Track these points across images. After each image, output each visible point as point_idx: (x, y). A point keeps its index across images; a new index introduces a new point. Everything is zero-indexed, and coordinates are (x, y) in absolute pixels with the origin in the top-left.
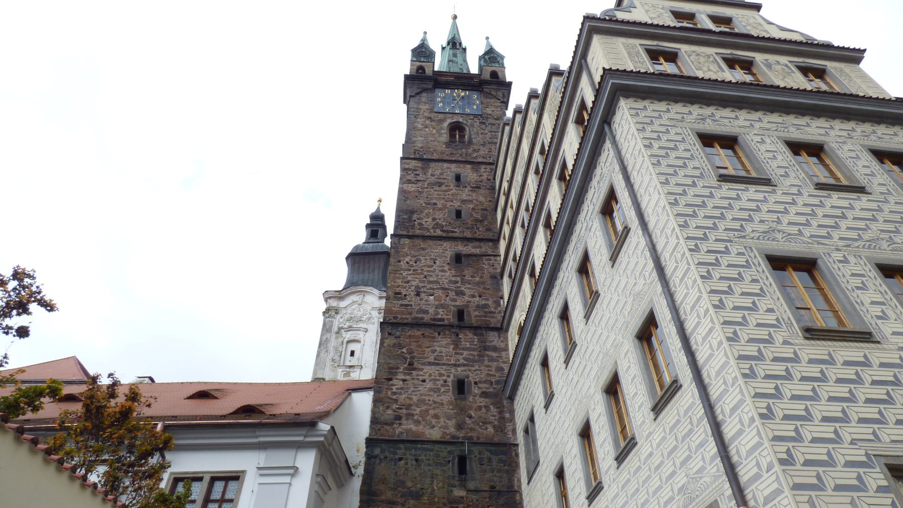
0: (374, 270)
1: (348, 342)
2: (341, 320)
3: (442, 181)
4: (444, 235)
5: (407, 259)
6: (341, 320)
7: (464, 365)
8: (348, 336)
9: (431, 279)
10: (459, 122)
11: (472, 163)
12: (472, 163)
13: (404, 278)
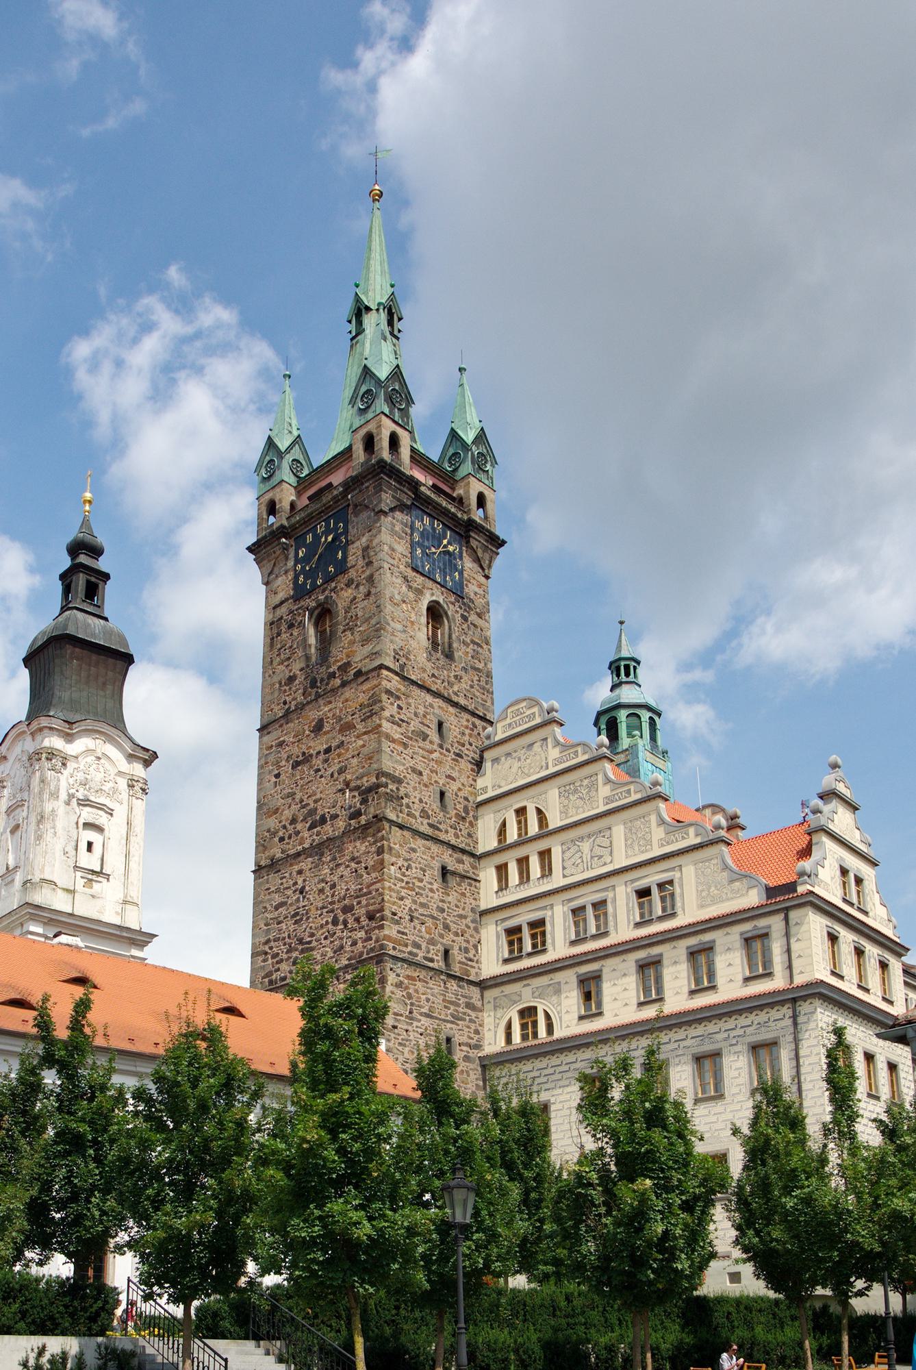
0: (104, 684)
1: (87, 825)
3: (425, 729)
4: (429, 831)
5: (400, 862)
6: (71, 781)
8: (87, 814)
10: (437, 602)
11: (456, 705)
12: (456, 705)
13: (398, 892)
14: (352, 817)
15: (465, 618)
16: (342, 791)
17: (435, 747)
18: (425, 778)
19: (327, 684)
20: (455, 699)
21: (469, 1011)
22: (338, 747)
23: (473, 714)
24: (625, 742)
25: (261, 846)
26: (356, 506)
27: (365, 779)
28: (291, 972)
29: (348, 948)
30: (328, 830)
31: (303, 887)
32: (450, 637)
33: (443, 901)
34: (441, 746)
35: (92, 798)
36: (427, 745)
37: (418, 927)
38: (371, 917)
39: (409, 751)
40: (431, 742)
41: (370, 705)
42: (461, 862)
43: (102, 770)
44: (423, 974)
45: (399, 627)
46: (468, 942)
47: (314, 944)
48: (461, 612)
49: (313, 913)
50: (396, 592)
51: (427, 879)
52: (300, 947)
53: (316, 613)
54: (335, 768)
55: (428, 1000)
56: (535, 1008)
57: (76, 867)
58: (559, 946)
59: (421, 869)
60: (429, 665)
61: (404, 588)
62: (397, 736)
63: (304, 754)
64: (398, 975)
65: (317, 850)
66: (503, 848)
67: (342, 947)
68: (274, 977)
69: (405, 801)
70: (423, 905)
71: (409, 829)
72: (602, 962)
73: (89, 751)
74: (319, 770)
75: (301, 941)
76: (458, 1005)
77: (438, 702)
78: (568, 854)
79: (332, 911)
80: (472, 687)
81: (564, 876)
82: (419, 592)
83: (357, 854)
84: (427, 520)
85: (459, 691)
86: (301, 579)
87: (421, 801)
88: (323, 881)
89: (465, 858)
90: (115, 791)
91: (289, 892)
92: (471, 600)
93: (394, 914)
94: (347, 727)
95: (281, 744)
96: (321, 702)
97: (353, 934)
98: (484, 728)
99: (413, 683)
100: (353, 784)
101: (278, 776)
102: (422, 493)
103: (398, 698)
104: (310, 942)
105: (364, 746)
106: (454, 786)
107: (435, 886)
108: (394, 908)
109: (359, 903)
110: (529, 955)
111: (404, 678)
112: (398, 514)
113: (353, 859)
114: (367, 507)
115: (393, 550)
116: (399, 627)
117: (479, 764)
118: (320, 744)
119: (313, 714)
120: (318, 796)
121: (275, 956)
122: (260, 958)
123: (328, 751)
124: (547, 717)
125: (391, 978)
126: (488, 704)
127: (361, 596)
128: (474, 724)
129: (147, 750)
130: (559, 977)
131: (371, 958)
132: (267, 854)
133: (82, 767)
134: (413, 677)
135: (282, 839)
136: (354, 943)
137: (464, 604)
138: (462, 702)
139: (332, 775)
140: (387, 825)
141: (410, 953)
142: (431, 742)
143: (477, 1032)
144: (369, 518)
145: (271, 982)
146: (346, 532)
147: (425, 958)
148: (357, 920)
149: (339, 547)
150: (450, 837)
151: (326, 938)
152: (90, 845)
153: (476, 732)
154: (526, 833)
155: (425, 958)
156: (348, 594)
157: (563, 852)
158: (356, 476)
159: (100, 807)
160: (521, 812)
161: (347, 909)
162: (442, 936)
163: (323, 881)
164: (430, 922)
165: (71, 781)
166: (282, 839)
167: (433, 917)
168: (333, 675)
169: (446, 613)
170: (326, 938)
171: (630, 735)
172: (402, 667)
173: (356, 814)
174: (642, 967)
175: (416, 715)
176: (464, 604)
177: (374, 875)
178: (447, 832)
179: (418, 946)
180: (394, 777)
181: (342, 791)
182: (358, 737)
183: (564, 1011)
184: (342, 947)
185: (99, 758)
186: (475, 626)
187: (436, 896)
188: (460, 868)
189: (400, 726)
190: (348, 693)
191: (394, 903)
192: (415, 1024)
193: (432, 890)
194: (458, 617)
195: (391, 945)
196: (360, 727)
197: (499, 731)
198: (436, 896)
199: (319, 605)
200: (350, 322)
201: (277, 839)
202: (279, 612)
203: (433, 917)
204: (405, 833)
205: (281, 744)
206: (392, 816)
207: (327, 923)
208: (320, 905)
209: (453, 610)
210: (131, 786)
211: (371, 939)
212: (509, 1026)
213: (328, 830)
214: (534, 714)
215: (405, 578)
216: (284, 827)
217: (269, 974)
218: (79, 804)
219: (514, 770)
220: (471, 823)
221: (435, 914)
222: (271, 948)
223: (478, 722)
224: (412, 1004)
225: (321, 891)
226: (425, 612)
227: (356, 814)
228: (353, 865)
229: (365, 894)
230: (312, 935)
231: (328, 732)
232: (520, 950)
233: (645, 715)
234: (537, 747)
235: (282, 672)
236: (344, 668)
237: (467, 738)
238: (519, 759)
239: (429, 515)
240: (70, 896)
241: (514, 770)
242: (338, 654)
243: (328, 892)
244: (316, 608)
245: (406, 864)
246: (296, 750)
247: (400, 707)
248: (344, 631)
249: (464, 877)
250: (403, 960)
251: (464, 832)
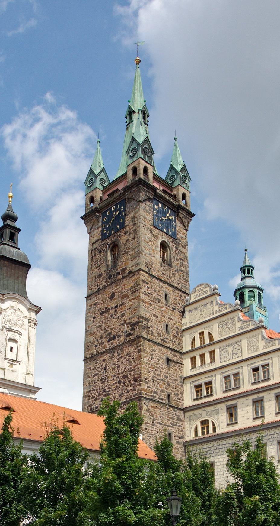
0: (18, 277)
1: (11, 340)
2: (3, 320)
3: (159, 297)
4: (161, 342)
7: (171, 427)
8: (11, 335)
9: (158, 373)
10: (165, 241)
11: (173, 286)
12: (173, 286)
13: (148, 369)
14: (127, 336)
15: (177, 248)
16: (123, 325)
17: (164, 305)
18: (159, 319)
19: (116, 277)
20: (173, 284)
21: (179, 422)
22: (121, 305)
23: (181, 291)
24: (247, 303)
25: (87, 349)
26: (129, 199)
27: (133, 319)
28: (100, 404)
29: (125, 394)
30: (117, 342)
31: (106, 367)
32: (170, 257)
33: (167, 373)
34: (166, 305)
35: (12, 328)
36: (160, 304)
37: (156, 384)
38: (135, 380)
39: (152, 307)
40: (162, 303)
41: (135, 287)
42: (175, 356)
43: (17, 315)
44: (158, 405)
45: (148, 252)
46: (178, 391)
47: (110, 392)
48: (175, 245)
49: (110, 378)
50: (147, 237)
51: (160, 363)
52: (104, 394)
53: (111, 246)
54: (120, 314)
55: (160, 417)
56: (208, 420)
57: (5, 358)
58: (218, 393)
59: (157, 359)
60: (161, 269)
61: (150, 235)
62: (147, 300)
63: (106, 308)
64: (147, 406)
65: (112, 351)
66: (194, 350)
67: (123, 393)
68: (93, 407)
69: (150, 329)
70: (158, 375)
71: (152, 341)
72: (237, 400)
73: (11, 307)
74: (112, 315)
75: (104, 391)
76: (174, 419)
77: (165, 285)
78: (222, 353)
79: (118, 378)
80: (180, 279)
81: (221, 362)
82: (157, 237)
83: (129, 353)
84: (160, 205)
85: (174, 280)
86: (105, 231)
87: (157, 329)
88: (114, 364)
89: (177, 354)
90: (23, 324)
91: (99, 369)
92: (180, 240)
93: (146, 379)
94: (125, 296)
95: (96, 304)
96: (113, 285)
97: (127, 388)
98: (185, 297)
99: (154, 277)
100: (127, 322)
101: (94, 318)
102: (158, 193)
103: (147, 284)
104: (108, 391)
105: (132, 305)
106: (172, 322)
107: (164, 367)
108: (146, 376)
109: (130, 374)
110: (205, 397)
111: (150, 275)
112: (147, 202)
113: (127, 355)
114: (134, 199)
115: (145, 218)
116: (148, 252)
117: (183, 313)
118: (113, 304)
119: (110, 291)
120: (112, 327)
121: (93, 397)
122: (87, 398)
123: (116, 307)
124: (213, 292)
125: (144, 407)
126: (187, 286)
127: (131, 238)
128: (181, 295)
129: (37, 307)
130: (218, 406)
131: (136, 398)
132: (90, 352)
133: (8, 314)
134: (154, 274)
135: (96, 346)
136: (128, 392)
137: (176, 242)
138: (176, 285)
139: (118, 318)
140: (142, 340)
141: (153, 396)
142: (162, 303)
143: (182, 431)
144: (135, 204)
145: (91, 409)
146: (124, 210)
147: (159, 398)
148: (129, 381)
149: (121, 217)
150: (170, 345)
151: (115, 390)
152: (12, 348)
153: (182, 299)
154: (204, 343)
155: (159, 398)
156: (125, 237)
157: (220, 352)
158: (129, 186)
159: (16, 332)
160: (202, 334)
161: (125, 377)
162: (167, 389)
163: (114, 364)
164: (161, 383)
165: (3, 320)
166: (96, 346)
167: (163, 380)
168: (119, 274)
169: (169, 246)
170: (115, 390)
171: (250, 300)
172: (149, 270)
173: (129, 335)
174: (255, 402)
175: (155, 291)
176: (176, 242)
177: (137, 362)
178: (169, 343)
179: (156, 393)
180: (146, 318)
181: (123, 325)
182: (130, 301)
183: (220, 422)
184: (123, 393)
185: (15, 310)
186: (181, 252)
187: (164, 371)
188: (175, 359)
189: (148, 296)
190: (125, 281)
191: (146, 374)
192: (155, 427)
193: (162, 368)
194: (174, 248)
195: (144, 393)
196: (131, 296)
197: (192, 298)
198: (164, 371)
199: (113, 243)
200: (126, 117)
201: (94, 346)
202: (95, 246)
203: (163, 380)
204: (151, 343)
205: (96, 304)
206: (145, 336)
207: (116, 383)
208: (113, 375)
209: (171, 245)
210: (30, 323)
211: (135, 390)
212: (196, 428)
213: (117, 342)
214: (207, 290)
215: (151, 231)
216: (97, 340)
217: (90, 405)
218: (7, 331)
219: (199, 315)
220: (179, 339)
221: (164, 379)
222: (91, 394)
223: (182, 294)
224: (153, 419)
225: (114, 369)
226: (159, 246)
227: (129, 335)
228: (128, 357)
229: (133, 370)
230: (110, 388)
231: (117, 299)
232: (201, 395)
233: (256, 291)
234: (208, 305)
235: (96, 272)
236: (124, 270)
237: (178, 301)
238: (201, 311)
239: (161, 203)
240: (3, 371)
241: (199, 315)
242: (121, 264)
243: (117, 369)
244: (111, 244)
245: (151, 357)
246: (102, 307)
247: (148, 288)
248: (124, 254)
249: (176, 363)
250: (150, 399)
251: (177, 343)
